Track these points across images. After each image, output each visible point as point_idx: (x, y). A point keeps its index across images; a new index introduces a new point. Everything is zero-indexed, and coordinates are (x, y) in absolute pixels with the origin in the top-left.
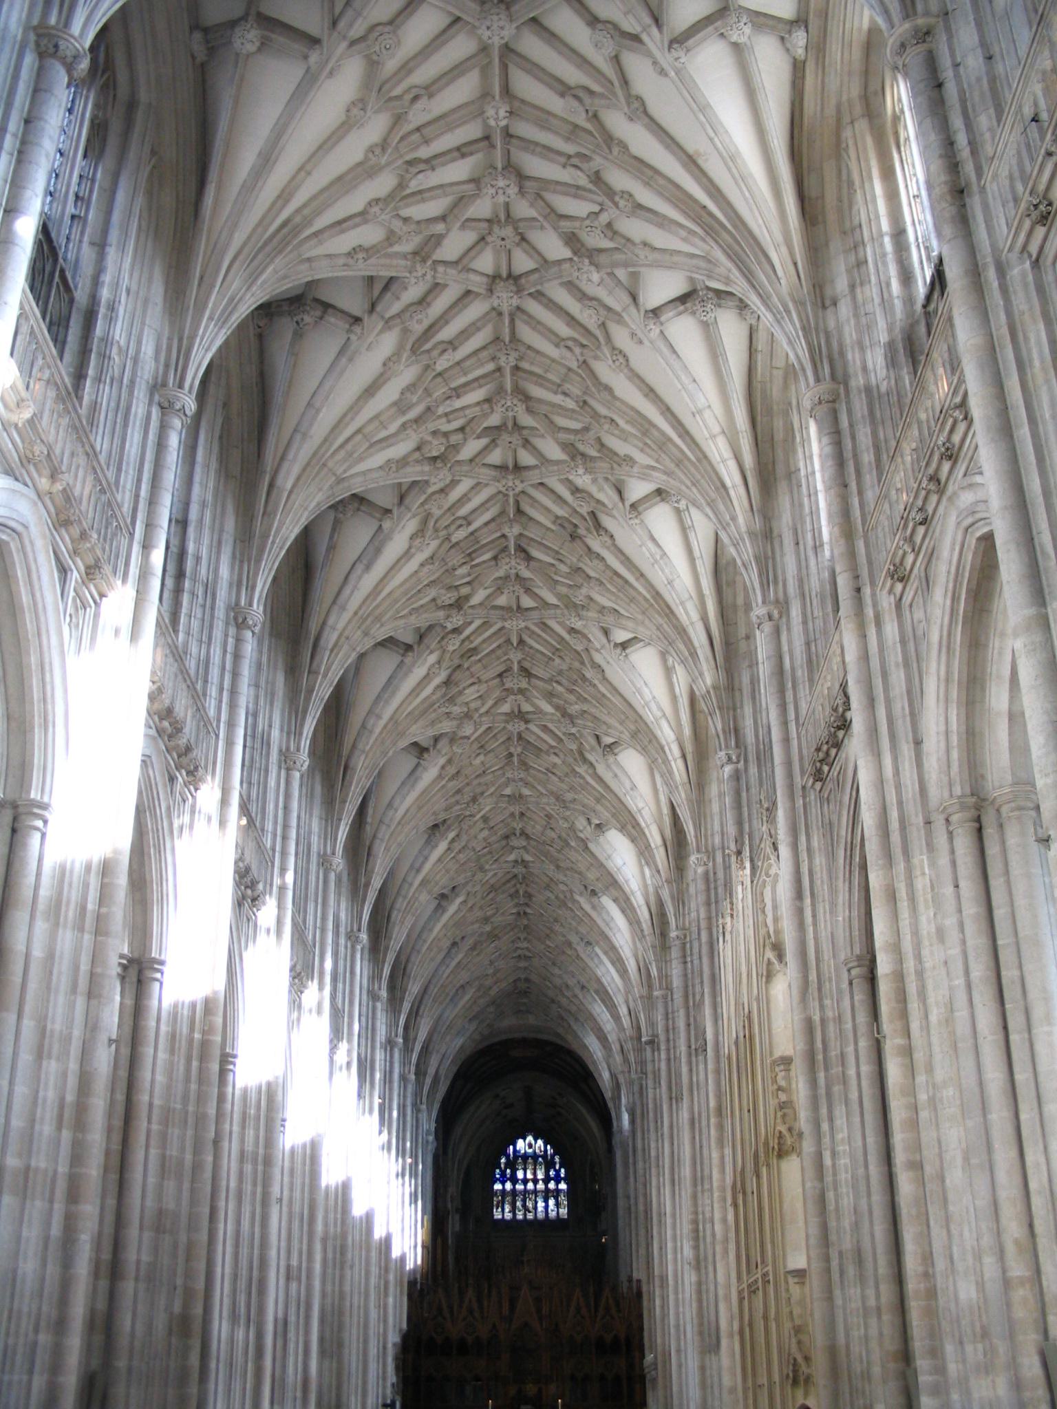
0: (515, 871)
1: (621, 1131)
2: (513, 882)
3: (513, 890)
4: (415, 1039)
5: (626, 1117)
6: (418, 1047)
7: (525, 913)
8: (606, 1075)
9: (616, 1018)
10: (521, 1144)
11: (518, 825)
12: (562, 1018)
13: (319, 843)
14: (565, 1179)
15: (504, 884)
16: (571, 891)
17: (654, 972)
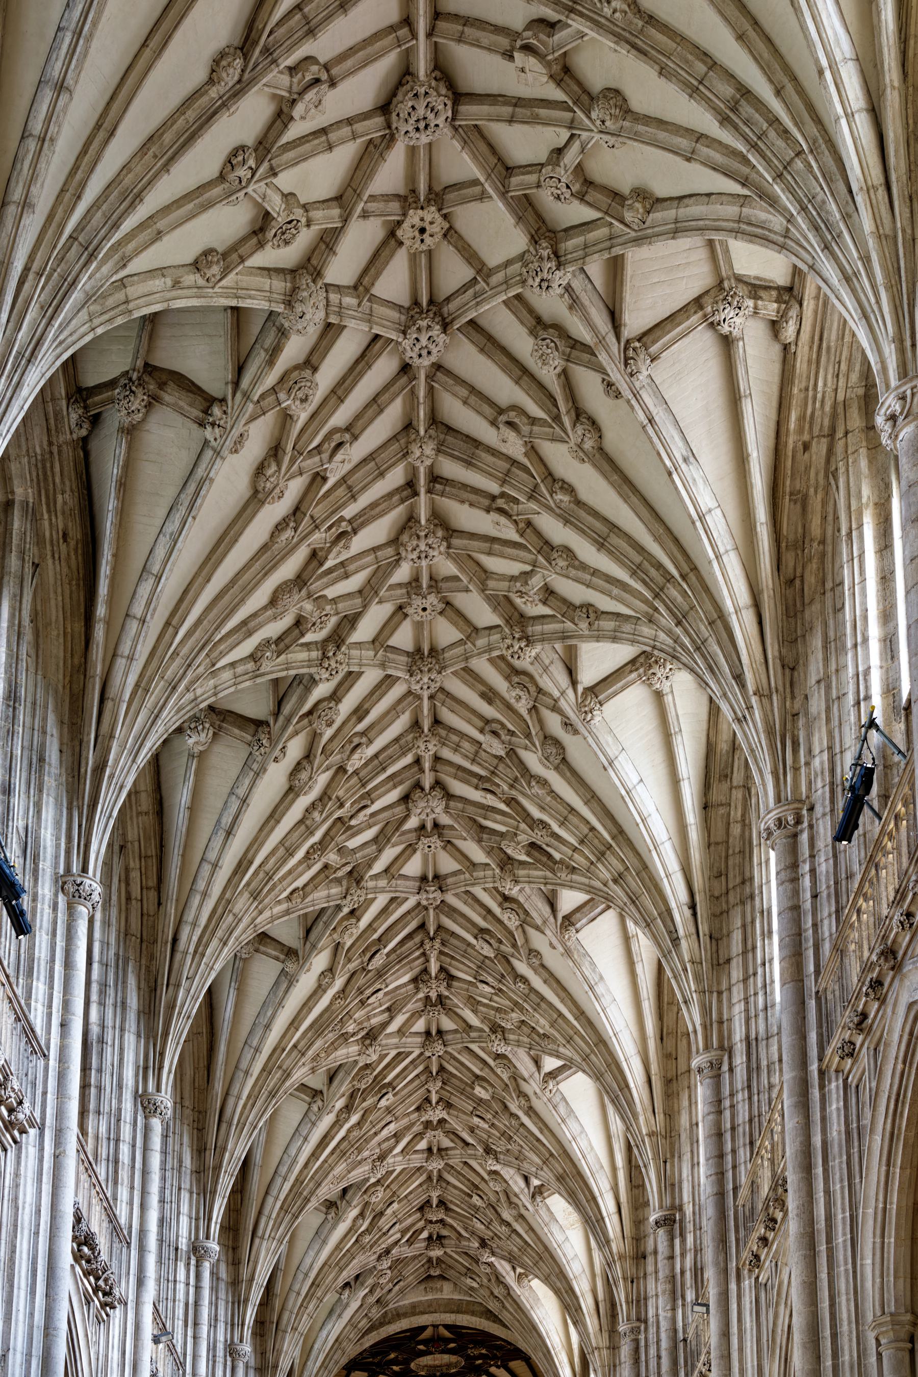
2: (417, 939)
7: (440, 1032)
16: (526, 920)
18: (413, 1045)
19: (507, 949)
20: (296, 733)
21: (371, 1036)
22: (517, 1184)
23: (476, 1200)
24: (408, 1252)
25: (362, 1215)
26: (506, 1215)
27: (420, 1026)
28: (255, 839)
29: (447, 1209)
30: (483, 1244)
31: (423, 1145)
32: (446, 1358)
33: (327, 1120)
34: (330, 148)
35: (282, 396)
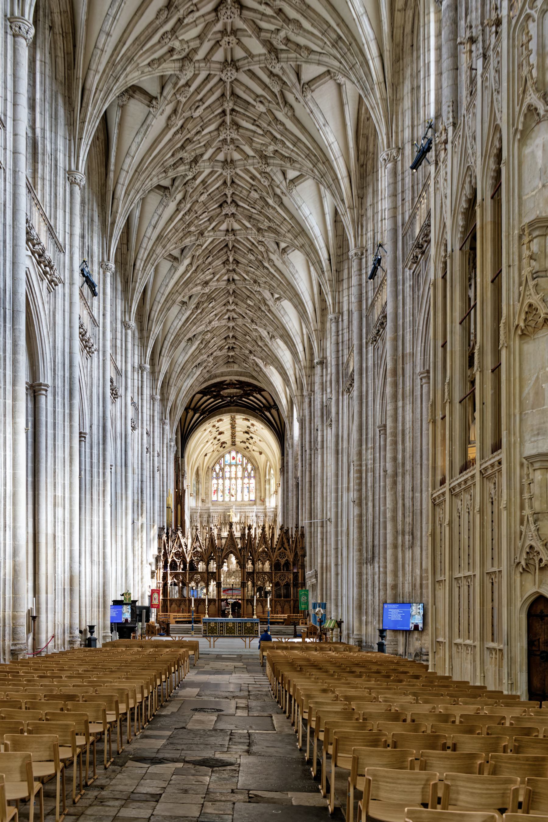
0: (227, 238)
1: (292, 438)
2: (225, 250)
3: (225, 258)
4: (160, 372)
5: (296, 426)
6: (161, 378)
7: (233, 280)
8: (284, 402)
9: (294, 353)
10: (227, 457)
11: (229, 192)
12: (257, 365)
13: (65, 160)
14: (254, 477)
15: (219, 252)
17: (329, 300)
18: (223, 284)
19: (260, 257)
20: (180, 192)
21: (206, 283)
22: (264, 334)
23: (247, 337)
24: (218, 353)
25: (201, 342)
26: (260, 343)
27: (226, 278)
28: (164, 228)
29: (236, 339)
30: (251, 352)
31: (226, 317)
32: (235, 390)
33: (189, 312)
34: (196, 26)
35: (178, 96)
